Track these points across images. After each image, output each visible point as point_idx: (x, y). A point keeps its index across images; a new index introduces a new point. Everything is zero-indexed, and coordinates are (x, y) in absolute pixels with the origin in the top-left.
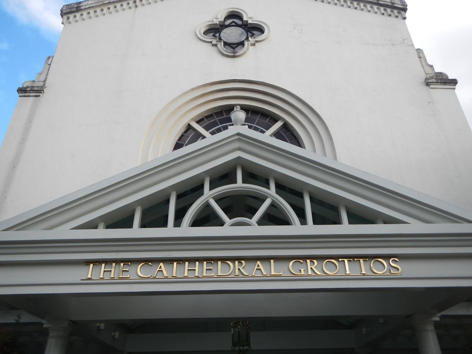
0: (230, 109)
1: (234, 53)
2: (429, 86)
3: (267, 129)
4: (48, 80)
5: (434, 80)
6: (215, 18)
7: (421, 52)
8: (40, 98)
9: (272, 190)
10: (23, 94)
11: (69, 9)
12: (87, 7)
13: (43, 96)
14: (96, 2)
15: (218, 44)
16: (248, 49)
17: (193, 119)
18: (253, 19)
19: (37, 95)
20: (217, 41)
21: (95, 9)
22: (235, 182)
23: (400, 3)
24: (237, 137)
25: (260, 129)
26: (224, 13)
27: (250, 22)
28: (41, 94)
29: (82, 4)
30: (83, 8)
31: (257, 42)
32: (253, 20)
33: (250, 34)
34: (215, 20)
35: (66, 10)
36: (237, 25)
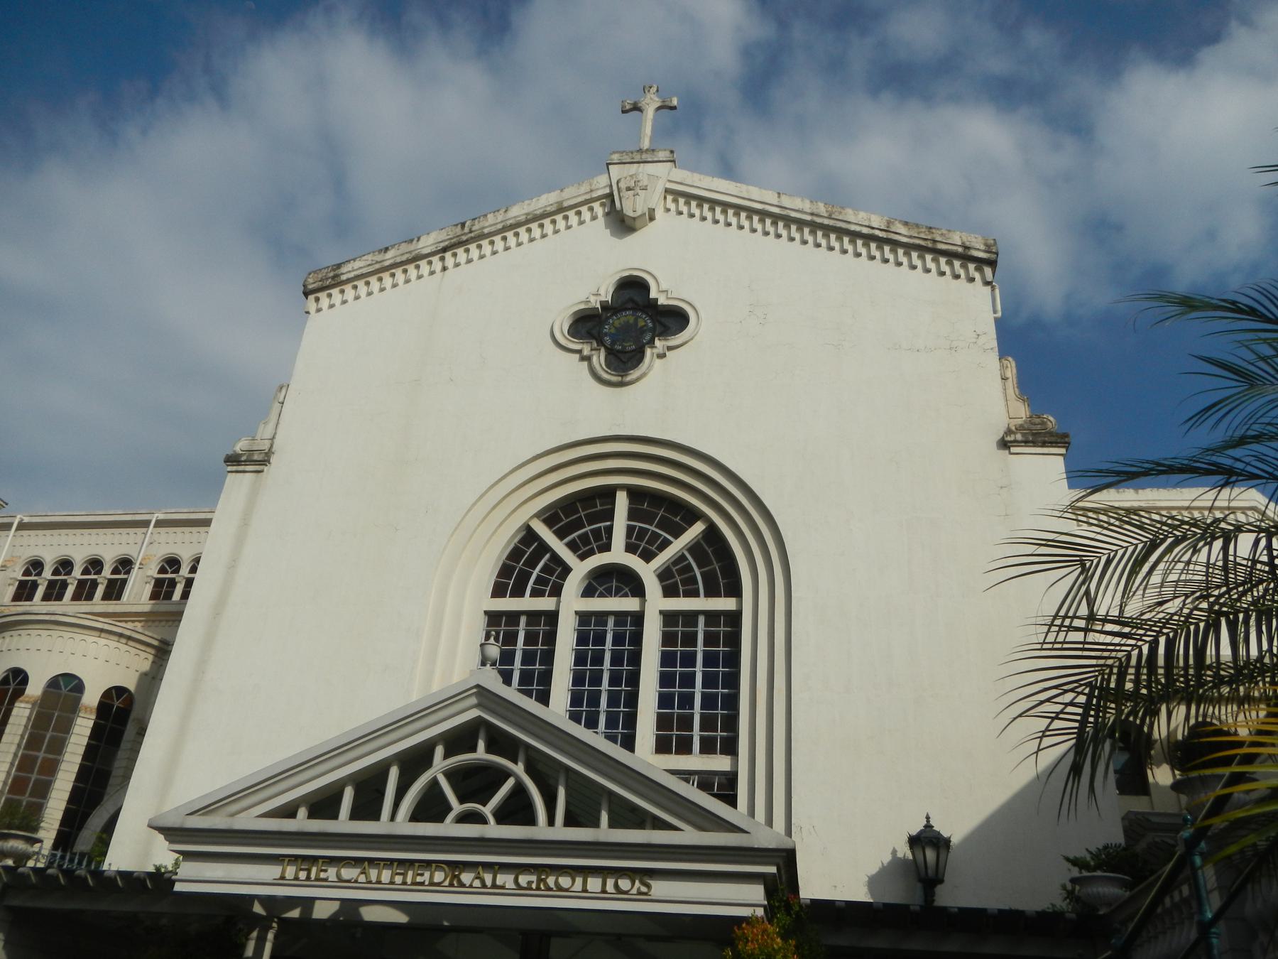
0: (608, 494)
1: (622, 376)
2: (1009, 448)
3: (676, 537)
4: (277, 436)
5: (1019, 437)
6: (593, 295)
7: (1009, 366)
8: (264, 473)
9: (519, 769)
10: (234, 468)
11: (320, 281)
12: (351, 275)
13: (268, 470)
14: (369, 265)
15: (592, 355)
16: (650, 367)
17: (537, 515)
18: (669, 293)
19: (259, 470)
20: (592, 350)
21: (367, 279)
22: (473, 749)
23: (982, 247)
24: (475, 690)
25: (662, 535)
26: (613, 282)
27: (662, 301)
28: (266, 469)
29: (344, 269)
30: (344, 277)
31: (670, 348)
32: (669, 296)
33: (659, 329)
34: (592, 299)
35: (314, 283)
36: (637, 307)
